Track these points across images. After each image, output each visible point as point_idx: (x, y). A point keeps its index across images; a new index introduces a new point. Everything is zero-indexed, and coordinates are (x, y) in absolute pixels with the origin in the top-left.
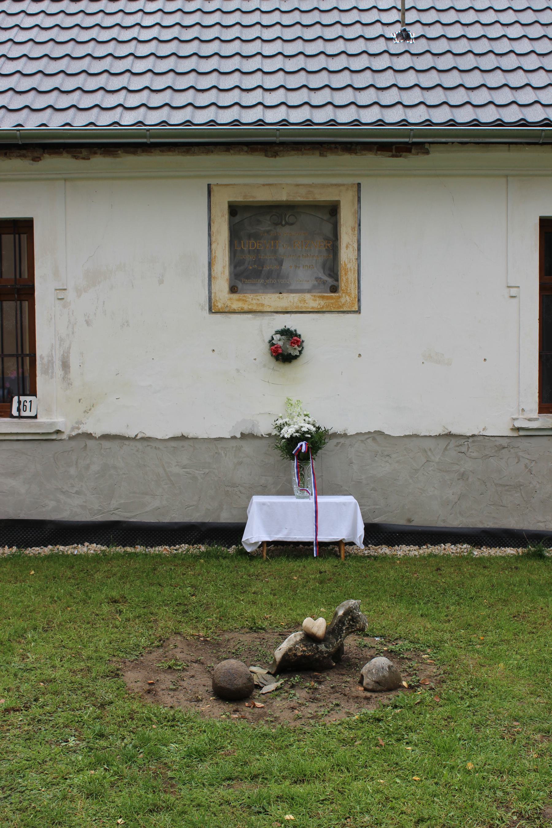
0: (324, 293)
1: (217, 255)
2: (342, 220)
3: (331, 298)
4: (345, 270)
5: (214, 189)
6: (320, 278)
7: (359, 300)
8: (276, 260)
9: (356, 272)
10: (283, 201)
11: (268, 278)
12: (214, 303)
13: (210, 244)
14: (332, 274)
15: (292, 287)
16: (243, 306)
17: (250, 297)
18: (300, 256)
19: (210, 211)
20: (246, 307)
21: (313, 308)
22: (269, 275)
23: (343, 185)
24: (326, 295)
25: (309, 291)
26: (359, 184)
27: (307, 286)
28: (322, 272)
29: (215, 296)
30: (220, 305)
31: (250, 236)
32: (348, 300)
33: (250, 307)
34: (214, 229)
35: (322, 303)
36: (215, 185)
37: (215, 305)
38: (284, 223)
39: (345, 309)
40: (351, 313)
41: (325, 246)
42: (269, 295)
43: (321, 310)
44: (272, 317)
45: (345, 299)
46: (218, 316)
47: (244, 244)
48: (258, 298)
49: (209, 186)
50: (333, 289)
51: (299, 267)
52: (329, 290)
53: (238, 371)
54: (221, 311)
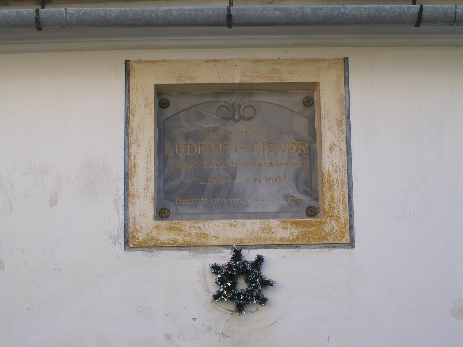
0: (298, 218)
1: (137, 162)
2: (322, 110)
3: (310, 224)
4: (329, 184)
5: (135, 67)
6: (292, 196)
7: (351, 228)
9: (346, 185)
10: (235, 84)
11: (214, 197)
12: (132, 233)
13: (127, 146)
14: (308, 189)
15: (250, 210)
16: (177, 237)
17: (186, 224)
18: (260, 165)
19: (129, 98)
20: (181, 239)
21: (282, 239)
23: (324, 60)
24: (302, 220)
25: (275, 215)
26: (346, 60)
27: (272, 208)
28: (294, 187)
29: (135, 224)
30: (141, 236)
31: (187, 136)
32: (336, 227)
33: (187, 239)
34: (134, 124)
35: (296, 231)
36: (136, 62)
37: (133, 237)
39: (331, 241)
40: (339, 247)
42: (216, 222)
43: (293, 242)
44: (221, 254)
45: (330, 226)
46: (138, 254)
47: (179, 148)
48: (200, 225)
49: (127, 63)
50: (312, 211)
51: (260, 181)
52: (304, 214)
53: (168, 337)
54: (143, 245)
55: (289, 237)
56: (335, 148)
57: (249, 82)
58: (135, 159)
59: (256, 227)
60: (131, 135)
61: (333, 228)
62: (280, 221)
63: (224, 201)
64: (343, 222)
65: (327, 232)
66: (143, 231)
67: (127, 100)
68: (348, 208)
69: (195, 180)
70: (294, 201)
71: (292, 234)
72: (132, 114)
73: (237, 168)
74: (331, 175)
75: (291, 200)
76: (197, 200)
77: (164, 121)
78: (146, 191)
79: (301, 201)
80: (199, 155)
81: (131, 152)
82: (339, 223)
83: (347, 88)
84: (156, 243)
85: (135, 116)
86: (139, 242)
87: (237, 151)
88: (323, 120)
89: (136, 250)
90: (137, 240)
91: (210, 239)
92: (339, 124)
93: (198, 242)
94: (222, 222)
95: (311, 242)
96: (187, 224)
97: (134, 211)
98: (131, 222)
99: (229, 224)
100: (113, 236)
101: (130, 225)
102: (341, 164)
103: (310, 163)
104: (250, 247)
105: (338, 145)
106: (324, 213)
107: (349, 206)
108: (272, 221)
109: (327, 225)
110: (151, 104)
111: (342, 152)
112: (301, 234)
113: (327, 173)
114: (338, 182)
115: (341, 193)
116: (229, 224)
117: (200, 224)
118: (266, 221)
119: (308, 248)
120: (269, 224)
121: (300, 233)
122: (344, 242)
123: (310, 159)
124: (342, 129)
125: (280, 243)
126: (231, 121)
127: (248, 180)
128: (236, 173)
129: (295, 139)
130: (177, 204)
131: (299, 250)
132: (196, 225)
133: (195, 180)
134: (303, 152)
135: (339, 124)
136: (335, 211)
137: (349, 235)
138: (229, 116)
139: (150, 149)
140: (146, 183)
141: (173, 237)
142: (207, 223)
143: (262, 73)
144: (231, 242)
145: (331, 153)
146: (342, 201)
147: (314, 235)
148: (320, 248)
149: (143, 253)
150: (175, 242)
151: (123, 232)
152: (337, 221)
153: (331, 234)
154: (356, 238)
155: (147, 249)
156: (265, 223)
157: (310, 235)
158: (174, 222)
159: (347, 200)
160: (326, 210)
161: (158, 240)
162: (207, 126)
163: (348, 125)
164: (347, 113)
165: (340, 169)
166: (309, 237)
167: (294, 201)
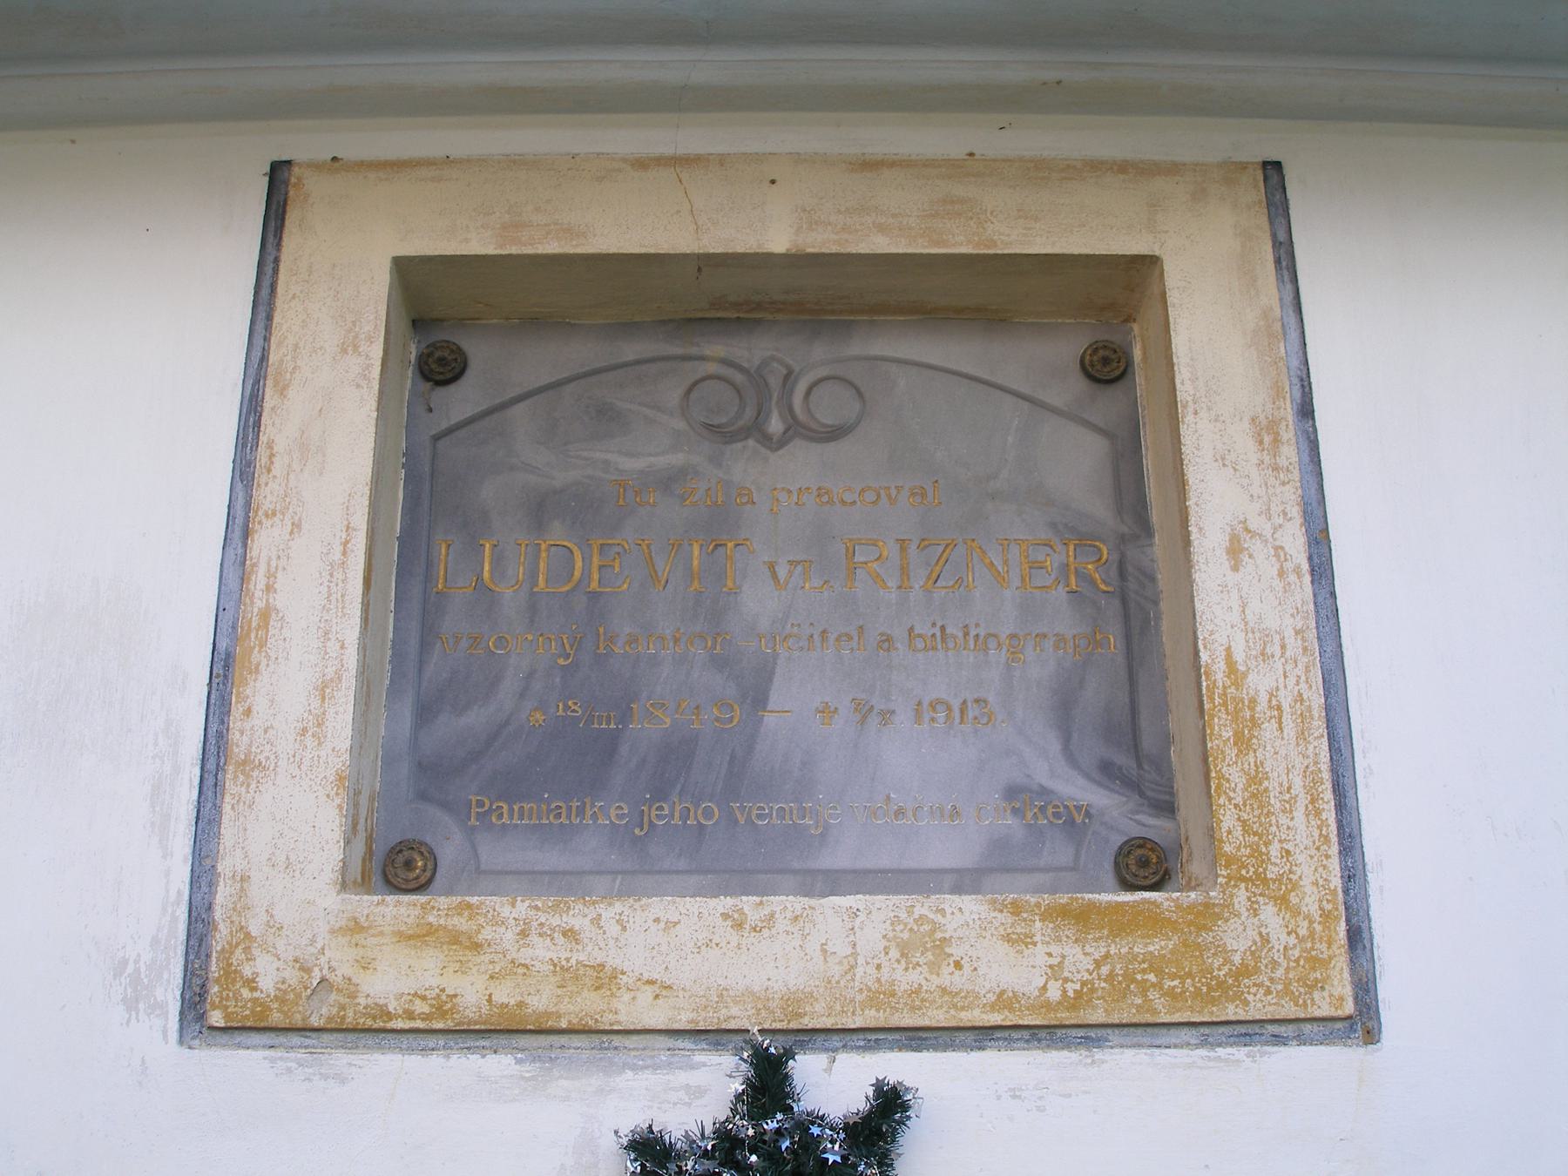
1: (280, 600)
3: (1154, 922)
4: (1236, 715)
5: (312, 190)
6: (1044, 791)
7: (1358, 938)
8: (720, 663)
9: (1319, 726)
11: (660, 794)
12: (227, 953)
13: (240, 527)
15: (838, 857)
16: (452, 983)
17: (506, 915)
18: (887, 641)
20: (473, 993)
21: (1004, 1000)
22: (671, 767)
24: (1105, 897)
25: (965, 881)
26: (1273, 169)
27: (947, 849)
28: (1055, 747)
29: (241, 905)
31: (539, 510)
32: (1279, 937)
33: (505, 994)
34: (278, 430)
35: (1079, 958)
36: (317, 166)
37: (230, 974)
38: (775, 425)
40: (1302, 1040)
41: (1065, 567)
42: (660, 907)
43: (1065, 1017)
44: (682, 1077)
45: (1249, 928)
46: (249, 1067)
47: (497, 561)
49: (278, 173)
50: (1144, 863)
51: (887, 716)
52: (1109, 877)
54: (276, 1018)
55: (1044, 988)
56: (1256, 546)
57: (834, 249)
58: (269, 588)
59: (872, 936)
60: (263, 480)
61: (1265, 939)
62: (994, 902)
63: (708, 813)
64: (1313, 909)
65: (1237, 959)
66: (281, 944)
67: (260, 326)
68: (1334, 838)
69: (567, 707)
70: (1057, 815)
71: (1055, 971)
72: (276, 384)
73: (775, 656)
74: (1245, 675)
75: (1042, 809)
76: (575, 804)
77: (436, 438)
78: (309, 741)
79: (1088, 814)
80: (594, 596)
81: (253, 552)
82: (1296, 912)
83: (1289, 286)
84: (343, 1008)
85: (291, 393)
86: (255, 1001)
87: (774, 576)
88: (1189, 418)
89: (239, 1046)
90: (246, 993)
91: (627, 997)
92: (1267, 439)
93: (563, 1008)
94: (692, 905)
95: (1155, 1012)
96: (506, 911)
97: (247, 839)
98: (223, 895)
99: (725, 916)
100: (130, 969)
101: (218, 914)
102: (1289, 621)
103: (1128, 637)
104: (836, 1041)
105: (1268, 532)
106: (1214, 864)
107: (1340, 827)
108: (951, 901)
109: (1234, 923)
110: (370, 340)
111: (1289, 565)
112: (1105, 970)
113: (1223, 666)
114: (1279, 708)
115: (1300, 763)
116: (725, 916)
117: (578, 917)
118: (923, 906)
119: (1140, 1046)
120: (939, 918)
121: (1098, 964)
122: (1325, 1010)
123: (1126, 617)
124: (1282, 462)
125: (995, 1019)
126: (751, 442)
127: (827, 712)
128: (770, 680)
129: (1053, 525)
130: (473, 821)
131: (1098, 1054)
132: (555, 921)
133: (567, 707)
134: (1093, 582)
135: (1267, 439)
136: (1274, 849)
137: (1346, 975)
138: (741, 423)
139: (346, 542)
140: (316, 703)
141: (434, 982)
142: (609, 912)
143: (894, 216)
144: (735, 1011)
145: (1235, 568)
146: (1303, 800)
147: (1173, 977)
148: (1204, 1043)
149: (273, 1060)
150: (443, 1004)
151: (181, 949)
152: (1282, 902)
153: (1257, 970)
154: (1387, 991)
155: (296, 1039)
156: (918, 911)
157: (1152, 977)
158: (443, 902)
159: (1329, 795)
160: (1227, 848)
161: (353, 996)
162: (639, 464)
163: (1305, 446)
164: (1297, 394)
165: (1283, 647)
166: (1144, 988)
167: (1057, 815)
